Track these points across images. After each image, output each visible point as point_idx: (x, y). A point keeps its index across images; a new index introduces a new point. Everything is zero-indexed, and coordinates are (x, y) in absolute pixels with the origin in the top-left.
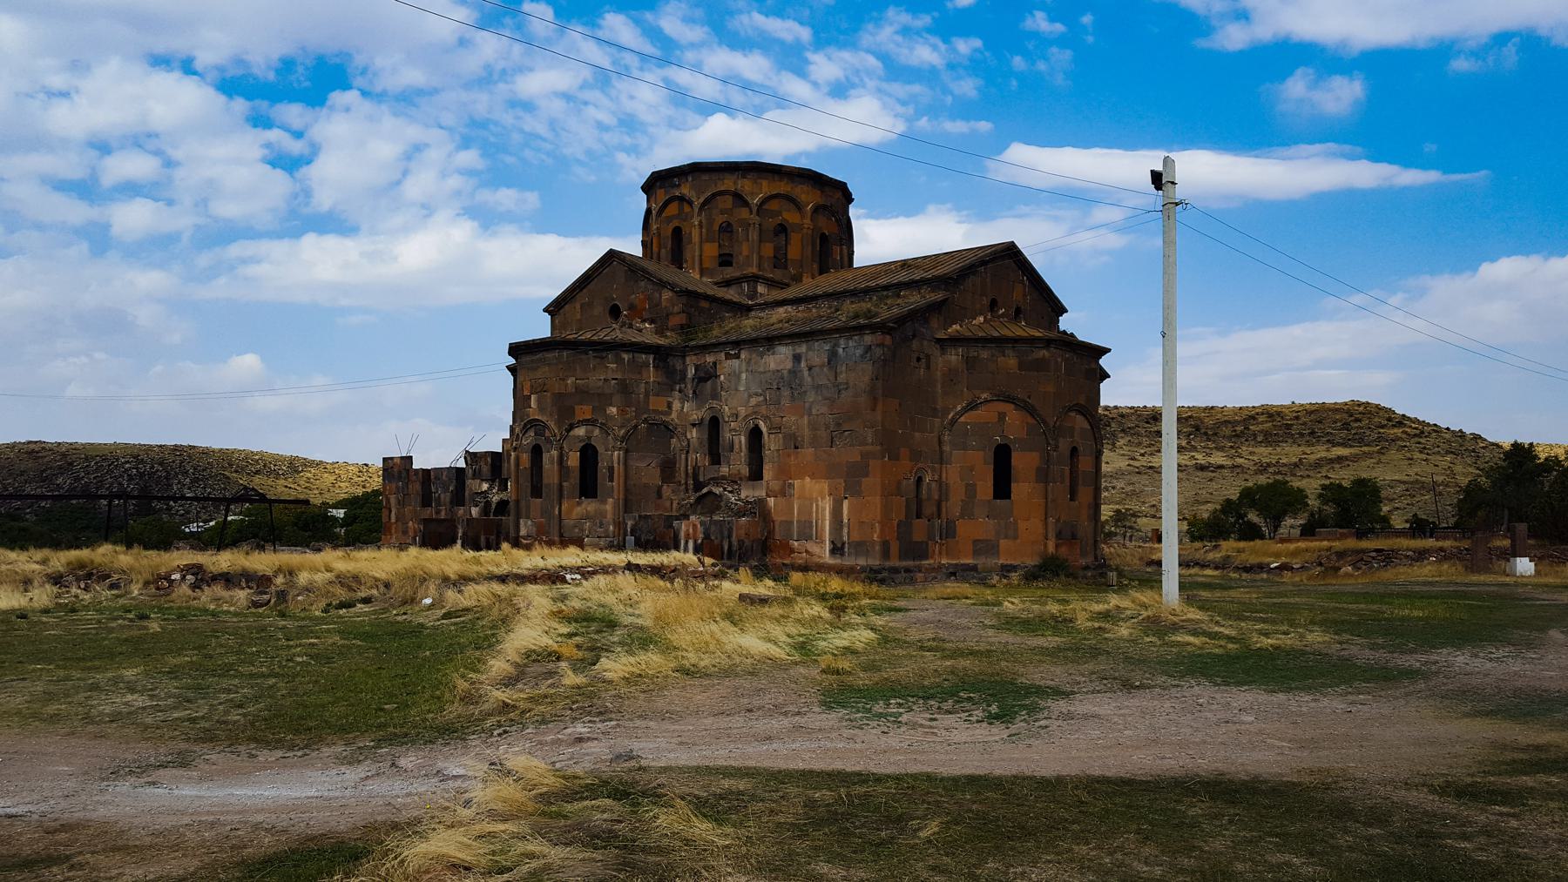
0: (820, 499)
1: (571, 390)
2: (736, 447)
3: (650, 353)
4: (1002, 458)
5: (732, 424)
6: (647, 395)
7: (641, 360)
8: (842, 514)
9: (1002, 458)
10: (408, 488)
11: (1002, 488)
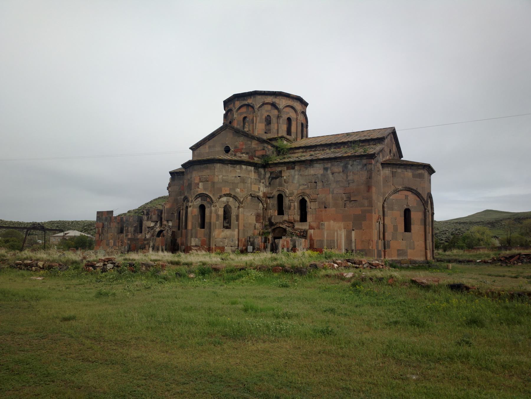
0: (339, 230)
1: (220, 181)
2: (292, 208)
3: (252, 166)
4: (407, 213)
5: (290, 197)
6: (251, 184)
7: (249, 169)
8: (351, 237)
9: (407, 213)
10: (110, 224)
11: (407, 228)
